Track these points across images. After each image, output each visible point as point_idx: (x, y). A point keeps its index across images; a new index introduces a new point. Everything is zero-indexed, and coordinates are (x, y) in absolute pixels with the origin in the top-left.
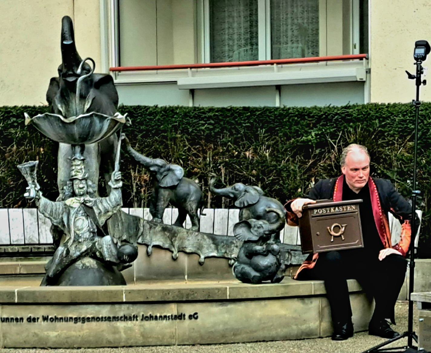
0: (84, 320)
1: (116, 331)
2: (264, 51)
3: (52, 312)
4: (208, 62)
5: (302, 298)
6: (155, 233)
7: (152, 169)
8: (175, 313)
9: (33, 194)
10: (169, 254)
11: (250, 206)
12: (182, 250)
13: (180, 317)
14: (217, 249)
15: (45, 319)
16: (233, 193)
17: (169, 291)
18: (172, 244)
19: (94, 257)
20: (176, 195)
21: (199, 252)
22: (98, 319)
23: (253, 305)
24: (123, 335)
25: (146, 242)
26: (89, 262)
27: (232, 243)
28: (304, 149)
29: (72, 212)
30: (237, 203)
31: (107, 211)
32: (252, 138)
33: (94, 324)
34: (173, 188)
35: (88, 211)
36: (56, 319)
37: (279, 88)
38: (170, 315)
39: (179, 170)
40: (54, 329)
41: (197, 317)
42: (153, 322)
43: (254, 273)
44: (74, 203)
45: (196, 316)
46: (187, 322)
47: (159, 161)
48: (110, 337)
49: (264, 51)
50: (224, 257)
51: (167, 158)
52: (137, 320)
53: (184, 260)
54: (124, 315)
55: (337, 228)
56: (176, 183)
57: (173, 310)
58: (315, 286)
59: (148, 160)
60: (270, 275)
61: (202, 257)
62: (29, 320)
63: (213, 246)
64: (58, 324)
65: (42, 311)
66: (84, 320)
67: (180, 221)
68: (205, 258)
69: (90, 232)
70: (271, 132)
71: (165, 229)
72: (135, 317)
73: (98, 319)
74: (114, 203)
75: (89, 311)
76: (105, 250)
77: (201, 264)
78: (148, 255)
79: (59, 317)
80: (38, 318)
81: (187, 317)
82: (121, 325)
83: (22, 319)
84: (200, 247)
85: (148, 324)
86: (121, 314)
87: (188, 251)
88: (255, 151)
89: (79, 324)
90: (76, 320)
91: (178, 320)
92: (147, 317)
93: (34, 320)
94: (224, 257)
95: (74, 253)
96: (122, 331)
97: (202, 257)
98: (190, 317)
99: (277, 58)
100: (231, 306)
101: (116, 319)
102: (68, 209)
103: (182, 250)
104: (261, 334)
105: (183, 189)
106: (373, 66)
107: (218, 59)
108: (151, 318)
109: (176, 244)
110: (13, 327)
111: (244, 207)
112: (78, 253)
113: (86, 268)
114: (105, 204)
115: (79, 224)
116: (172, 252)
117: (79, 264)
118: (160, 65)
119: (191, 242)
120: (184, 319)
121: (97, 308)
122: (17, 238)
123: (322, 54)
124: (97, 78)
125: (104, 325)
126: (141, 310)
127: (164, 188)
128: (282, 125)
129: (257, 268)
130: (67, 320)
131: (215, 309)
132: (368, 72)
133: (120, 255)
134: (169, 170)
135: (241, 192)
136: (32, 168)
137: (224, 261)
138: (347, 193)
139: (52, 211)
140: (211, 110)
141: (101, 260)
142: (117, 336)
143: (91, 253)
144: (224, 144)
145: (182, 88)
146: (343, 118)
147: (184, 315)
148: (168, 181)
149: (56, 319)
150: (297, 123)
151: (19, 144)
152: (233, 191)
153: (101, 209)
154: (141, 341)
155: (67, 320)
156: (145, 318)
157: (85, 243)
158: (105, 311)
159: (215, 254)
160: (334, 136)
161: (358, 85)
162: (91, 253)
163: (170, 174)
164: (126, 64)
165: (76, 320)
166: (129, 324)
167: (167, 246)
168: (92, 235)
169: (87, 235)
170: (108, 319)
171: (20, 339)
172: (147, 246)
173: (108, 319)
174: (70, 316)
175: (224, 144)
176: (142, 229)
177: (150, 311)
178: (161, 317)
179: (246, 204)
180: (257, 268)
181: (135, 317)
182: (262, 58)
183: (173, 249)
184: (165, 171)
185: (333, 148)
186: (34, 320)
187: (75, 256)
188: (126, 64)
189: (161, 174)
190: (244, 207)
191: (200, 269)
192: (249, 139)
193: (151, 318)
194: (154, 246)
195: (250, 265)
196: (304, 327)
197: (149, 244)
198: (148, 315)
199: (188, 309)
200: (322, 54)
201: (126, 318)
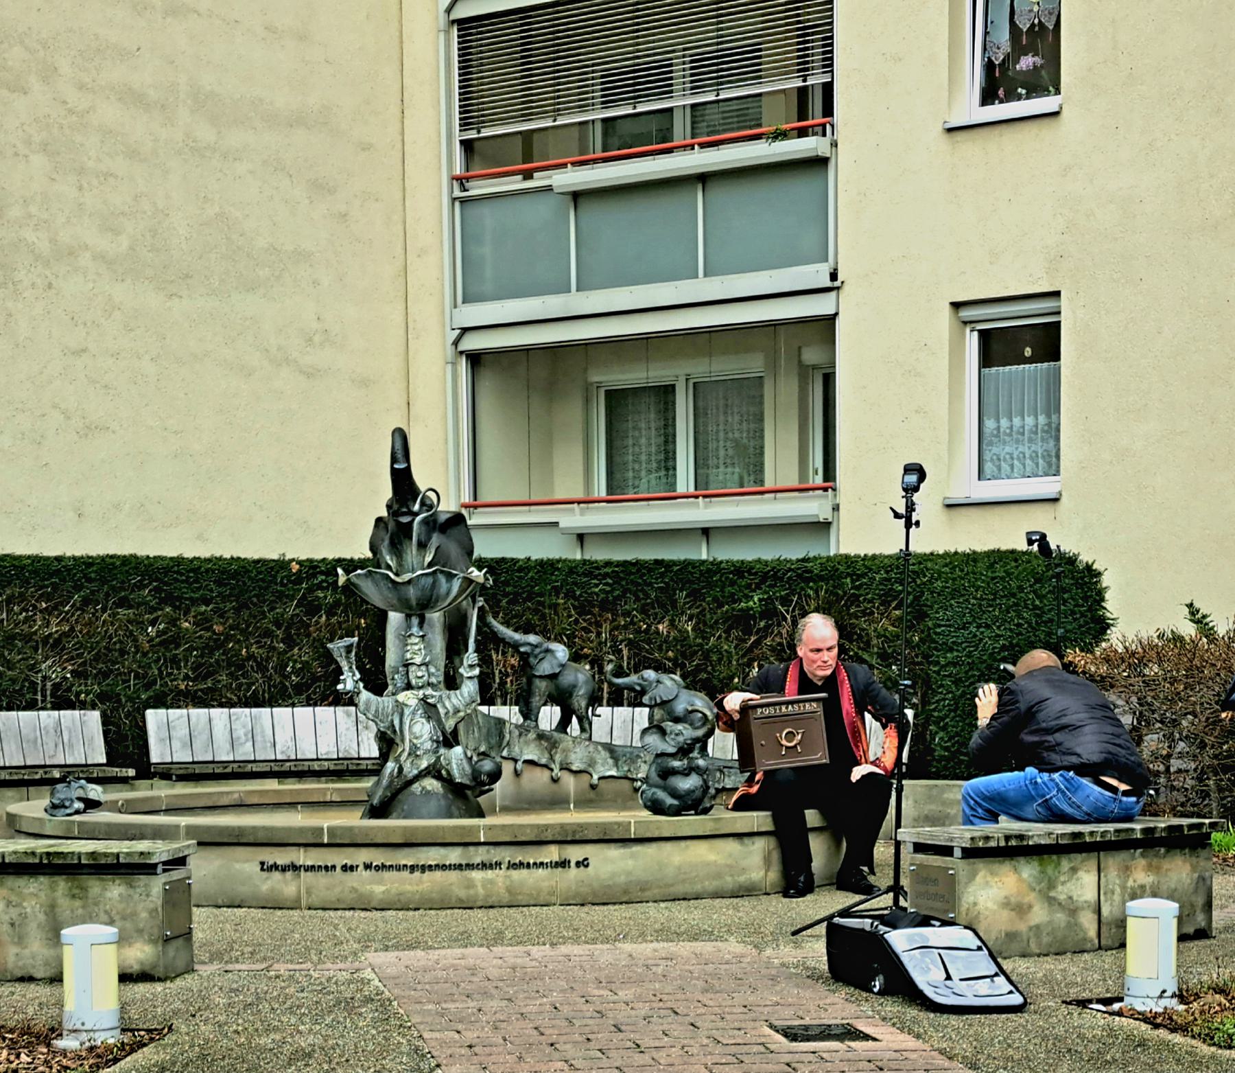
0: (423, 869)
1: (470, 885)
2: (685, 480)
3: (377, 857)
4: (603, 494)
5: (739, 836)
6: (527, 743)
7: (522, 649)
8: (556, 858)
9: (350, 685)
10: (547, 773)
11: (664, 704)
12: (565, 768)
13: (564, 864)
14: (616, 765)
15: (368, 867)
16: (639, 685)
17: (546, 827)
18: (552, 758)
19: (438, 777)
20: (557, 687)
21: (590, 770)
22: (444, 867)
23: (668, 846)
24: (481, 891)
25: (514, 755)
26: (431, 784)
27: (638, 756)
28: (743, 621)
29: (407, 712)
30: (646, 700)
32: (667, 605)
33: (438, 874)
34: (553, 677)
35: (430, 710)
37: (706, 532)
39: (561, 652)
40: (380, 882)
42: (525, 872)
43: (670, 801)
44: (409, 698)
46: (573, 872)
47: (532, 638)
48: (463, 894)
49: (685, 480)
50: (626, 778)
51: (545, 633)
53: (569, 782)
55: (790, 736)
56: (557, 670)
57: (552, 853)
58: (759, 819)
59: (517, 636)
60: (694, 804)
61: (595, 777)
62: (345, 868)
63: (610, 761)
64: (387, 875)
65: (363, 856)
66: (423, 869)
67: (563, 725)
68: (600, 778)
69: (433, 741)
70: (695, 596)
71: (541, 736)
73: (444, 867)
74: (468, 700)
75: (432, 856)
76: (455, 766)
77: (593, 787)
78: (517, 774)
79: (388, 864)
81: (573, 864)
82: (477, 875)
83: (334, 867)
84: (592, 763)
85: (516, 875)
86: (478, 860)
87: (574, 768)
88: (672, 624)
89: (417, 874)
90: (413, 868)
91: (560, 869)
93: (352, 868)
94: (626, 778)
95: (410, 771)
96: (479, 885)
97: (595, 777)
98: (578, 864)
99: (704, 489)
100: (637, 849)
101: (470, 866)
102: (400, 708)
103: (565, 768)
104: (680, 889)
105: (567, 679)
106: (842, 499)
107: (617, 490)
108: (521, 865)
109: (558, 758)
110: (321, 879)
111: (656, 705)
112: (415, 772)
113: (427, 793)
114: (455, 701)
115: (417, 729)
116: (552, 770)
117: (416, 787)
118: (534, 498)
119: (579, 755)
121: (442, 851)
122: (327, 749)
123: (769, 483)
124: (443, 518)
125: (454, 875)
126: (506, 855)
127: (540, 677)
128: (711, 586)
129: (674, 793)
130: (399, 868)
131: (614, 852)
132: (836, 508)
133: (476, 774)
134: (548, 651)
135: (651, 683)
136: (349, 649)
137: (626, 783)
138: (806, 685)
139: (377, 711)
140: (608, 563)
141: (448, 781)
142: (472, 892)
143: (434, 771)
144: (627, 614)
145: (565, 532)
146: (799, 576)
148: (545, 668)
150: (733, 584)
151: (330, 614)
152: (640, 681)
154: (506, 899)
155: (399, 868)
156: (513, 866)
158: (454, 856)
159: (613, 773)
160: (785, 601)
161: (822, 527)
162: (434, 771)
163: (549, 656)
164: (484, 497)
165: (413, 868)
166: (490, 874)
167: (543, 761)
169: (428, 745)
170: (459, 867)
171: (331, 896)
172: (516, 761)
173: (459, 867)
174: (403, 862)
175: (627, 614)
176: (507, 736)
177: (519, 855)
178: (535, 864)
179: (658, 701)
180: (674, 793)
182: (681, 488)
183: (553, 766)
185: (785, 619)
186: (352, 868)
187: (410, 776)
188: (484, 497)
189: (536, 657)
190: (656, 705)
191: (592, 795)
192: (662, 606)
193: (521, 865)
194: (526, 762)
195: (665, 789)
196: (742, 879)
198: (517, 861)
199: (575, 853)
200: (769, 483)
201: (484, 866)
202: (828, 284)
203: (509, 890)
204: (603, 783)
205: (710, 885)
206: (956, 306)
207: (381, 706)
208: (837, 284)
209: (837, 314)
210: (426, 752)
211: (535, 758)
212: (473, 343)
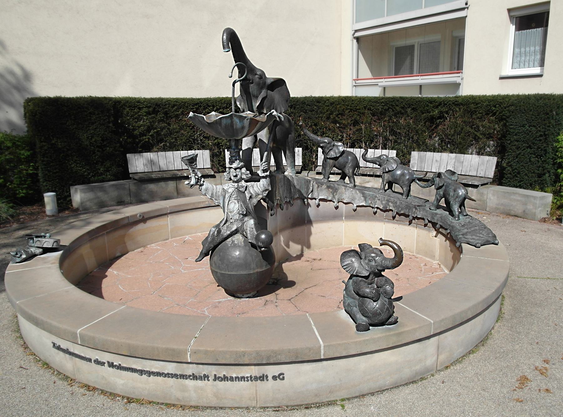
0: (150, 373)
1: (184, 389)
6: (321, 190)
13: (263, 378)
14: (365, 200)
18: (334, 197)
21: (353, 202)
25: (314, 196)
27: (376, 197)
29: (227, 196)
33: (160, 379)
36: (120, 367)
38: (249, 375)
41: (284, 378)
45: (281, 377)
48: (179, 395)
52: (209, 380)
54: (193, 374)
63: (363, 198)
66: (150, 373)
72: (206, 377)
74: (263, 189)
76: (248, 232)
80: (105, 363)
81: (270, 378)
82: (189, 383)
84: (354, 199)
86: (189, 372)
87: (345, 201)
90: (141, 372)
92: (219, 377)
97: (355, 205)
98: (274, 378)
101: (183, 376)
108: (225, 378)
109: (337, 197)
112: (229, 232)
114: (256, 189)
115: (232, 206)
119: (347, 195)
120: (268, 380)
124: (269, 82)
127: (330, 158)
142: (186, 394)
145: (380, 86)
146: (453, 103)
147: (267, 377)
149: (120, 367)
150: (428, 106)
157: (236, 223)
158: (170, 368)
159: (364, 204)
164: (360, 78)
165: (141, 372)
166: (199, 383)
167: (330, 199)
168: (241, 216)
169: (237, 217)
177: (223, 371)
178: (236, 378)
181: (206, 377)
183: (334, 201)
185: (447, 119)
188: (360, 78)
189: (328, 148)
193: (225, 378)
196: (418, 367)
201: (194, 377)
202: (465, 6)
203: (216, 395)
205: (389, 381)
206: (509, 10)
207: (215, 191)
208: (467, 6)
209: (466, 16)
210: (236, 220)
212: (357, 34)
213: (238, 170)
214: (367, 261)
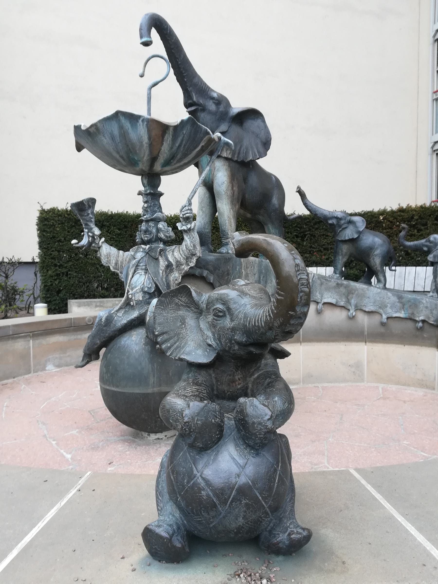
7: (330, 222)
12: (358, 309)
16: (426, 246)
18: (348, 301)
21: (381, 311)
30: (430, 258)
31: (179, 264)
34: (352, 241)
50: (411, 319)
53: (363, 320)
56: (356, 236)
68: (388, 318)
69: (145, 292)
77: (383, 324)
78: (319, 312)
84: (383, 306)
94: (411, 319)
97: (384, 317)
109: (353, 301)
114: (176, 254)
116: (349, 310)
137: (410, 324)
139: (116, 264)
152: (428, 244)
153: (171, 260)
159: (402, 315)
167: (342, 304)
168: (147, 297)
169: (139, 297)
172: (318, 303)
183: (350, 308)
184: (345, 223)
189: (340, 226)
191: (382, 330)
194: (325, 303)
197: (319, 301)
204: (391, 322)
210: (139, 303)
211: (334, 301)
213: (151, 224)
214: (210, 318)
